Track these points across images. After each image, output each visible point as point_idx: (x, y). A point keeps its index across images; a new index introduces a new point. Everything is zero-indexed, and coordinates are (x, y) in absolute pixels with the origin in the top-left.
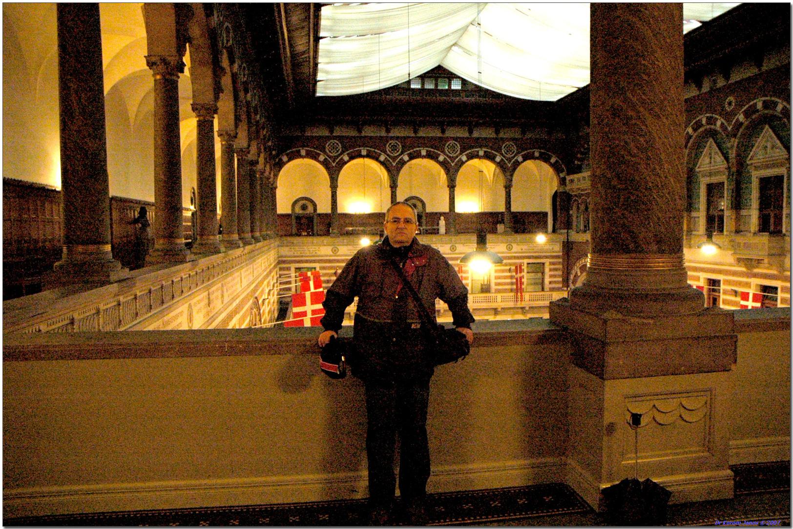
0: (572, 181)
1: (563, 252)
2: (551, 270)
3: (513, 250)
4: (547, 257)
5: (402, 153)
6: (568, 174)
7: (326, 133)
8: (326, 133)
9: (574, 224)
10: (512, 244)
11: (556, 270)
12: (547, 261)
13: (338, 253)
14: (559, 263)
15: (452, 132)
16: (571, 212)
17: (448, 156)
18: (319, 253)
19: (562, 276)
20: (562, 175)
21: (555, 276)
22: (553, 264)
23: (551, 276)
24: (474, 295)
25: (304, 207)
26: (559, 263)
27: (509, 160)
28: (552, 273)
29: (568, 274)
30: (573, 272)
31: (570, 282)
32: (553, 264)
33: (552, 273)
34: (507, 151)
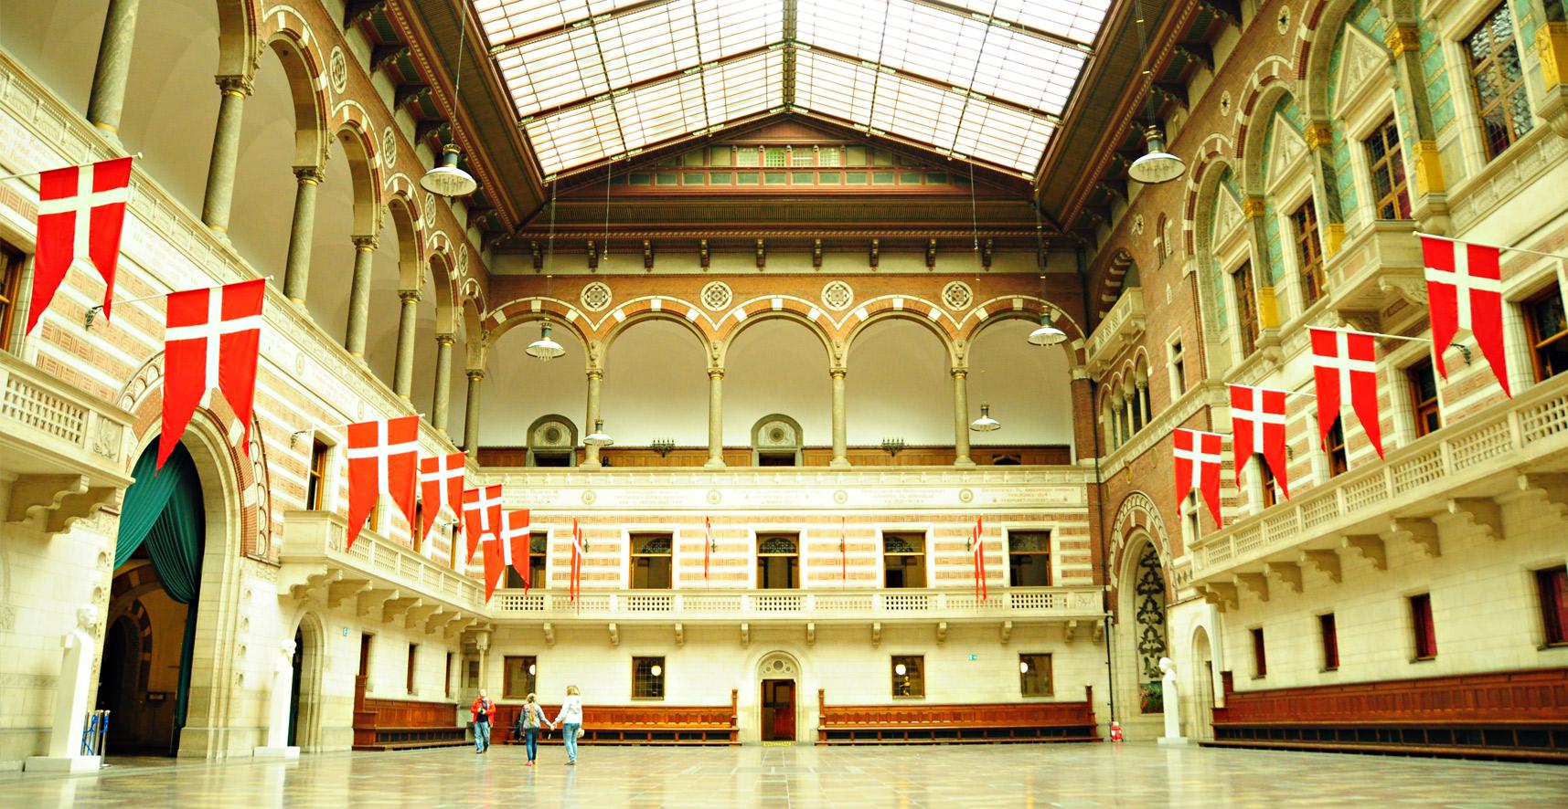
0: (1092, 351)
1: (1090, 506)
2: (1063, 545)
3: (973, 503)
4: (1052, 517)
5: (733, 305)
6: (1088, 336)
7: (586, 271)
8: (586, 271)
9: (1109, 441)
10: (974, 490)
11: (1077, 545)
12: (1055, 527)
13: (583, 490)
14: (1082, 531)
15: (831, 265)
16: (1101, 419)
17: (830, 312)
18: (555, 503)
19: (1094, 560)
20: (1076, 345)
21: (1073, 559)
22: (1069, 531)
23: (1065, 560)
25: (552, 435)
26: (1082, 531)
27: (959, 316)
28: (1068, 553)
29: (1105, 554)
30: (1113, 548)
31: (1111, 570)
32: (1069, 531)
33: (1068, 553)
34: (954, 299)
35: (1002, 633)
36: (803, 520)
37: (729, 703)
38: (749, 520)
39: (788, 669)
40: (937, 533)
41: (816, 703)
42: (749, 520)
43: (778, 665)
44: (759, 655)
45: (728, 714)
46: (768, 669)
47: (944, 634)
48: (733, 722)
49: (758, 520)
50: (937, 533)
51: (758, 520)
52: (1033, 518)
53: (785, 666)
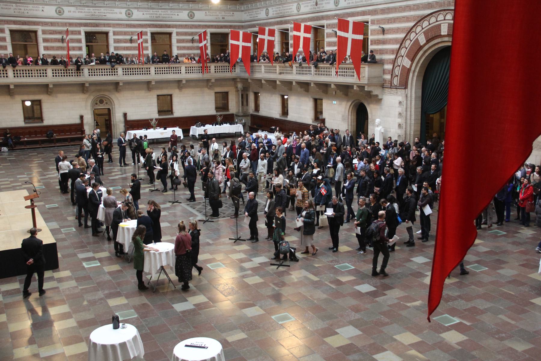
24: (157, 66)
35: (207, 83)
36: (109, 25)
37: (78, 121)
38: (81, 25)
39: (107, 103)
40: (178, 34)
41: (122, 119)
42: (81, 25)
43: (101, 102)
44: (92, 97)
45: (79, 128)
46: (96, 104)
47: (179, 84)
48: (83, 132)
49: (86, 25)
50: (178, 34)
51: (86, 25)
52: (221, 27)
53: (105, 102)
